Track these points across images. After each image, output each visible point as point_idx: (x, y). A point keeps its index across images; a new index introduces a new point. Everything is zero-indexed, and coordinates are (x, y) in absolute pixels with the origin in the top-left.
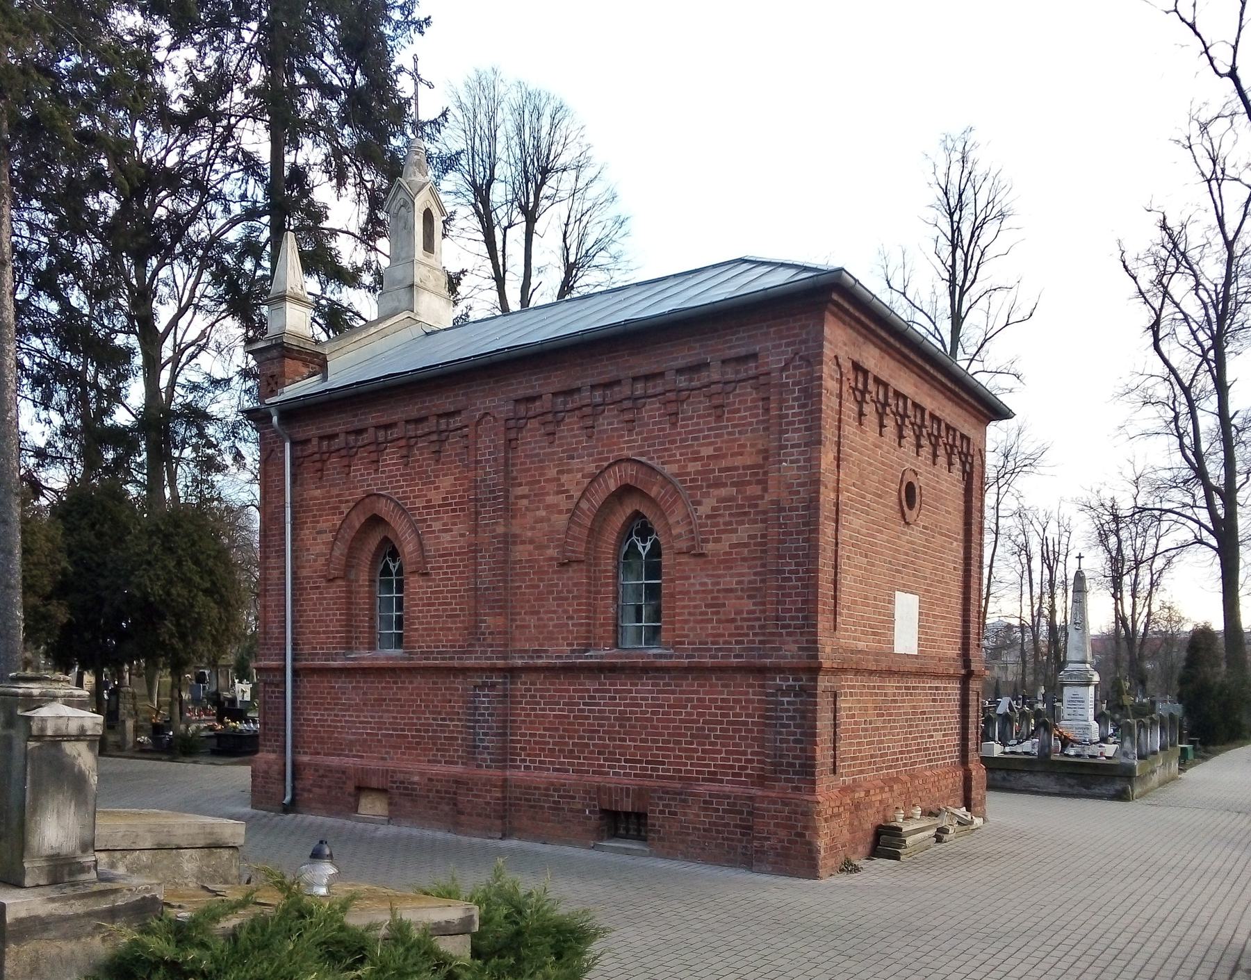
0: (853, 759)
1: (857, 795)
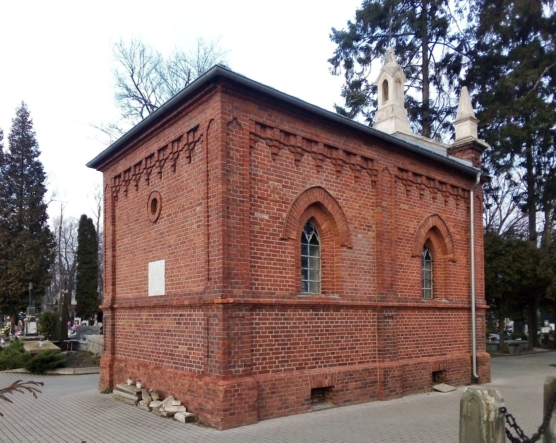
0: (125, 348)
1: (121, 364)
